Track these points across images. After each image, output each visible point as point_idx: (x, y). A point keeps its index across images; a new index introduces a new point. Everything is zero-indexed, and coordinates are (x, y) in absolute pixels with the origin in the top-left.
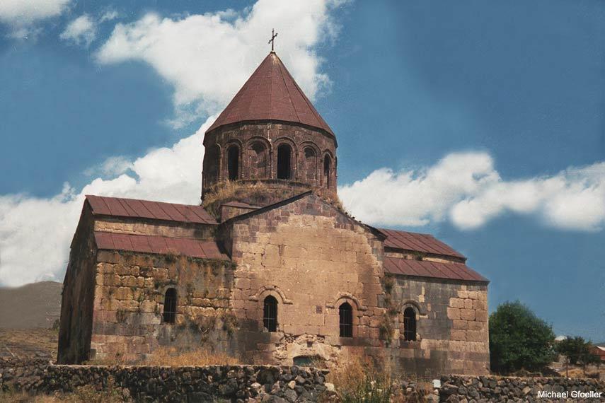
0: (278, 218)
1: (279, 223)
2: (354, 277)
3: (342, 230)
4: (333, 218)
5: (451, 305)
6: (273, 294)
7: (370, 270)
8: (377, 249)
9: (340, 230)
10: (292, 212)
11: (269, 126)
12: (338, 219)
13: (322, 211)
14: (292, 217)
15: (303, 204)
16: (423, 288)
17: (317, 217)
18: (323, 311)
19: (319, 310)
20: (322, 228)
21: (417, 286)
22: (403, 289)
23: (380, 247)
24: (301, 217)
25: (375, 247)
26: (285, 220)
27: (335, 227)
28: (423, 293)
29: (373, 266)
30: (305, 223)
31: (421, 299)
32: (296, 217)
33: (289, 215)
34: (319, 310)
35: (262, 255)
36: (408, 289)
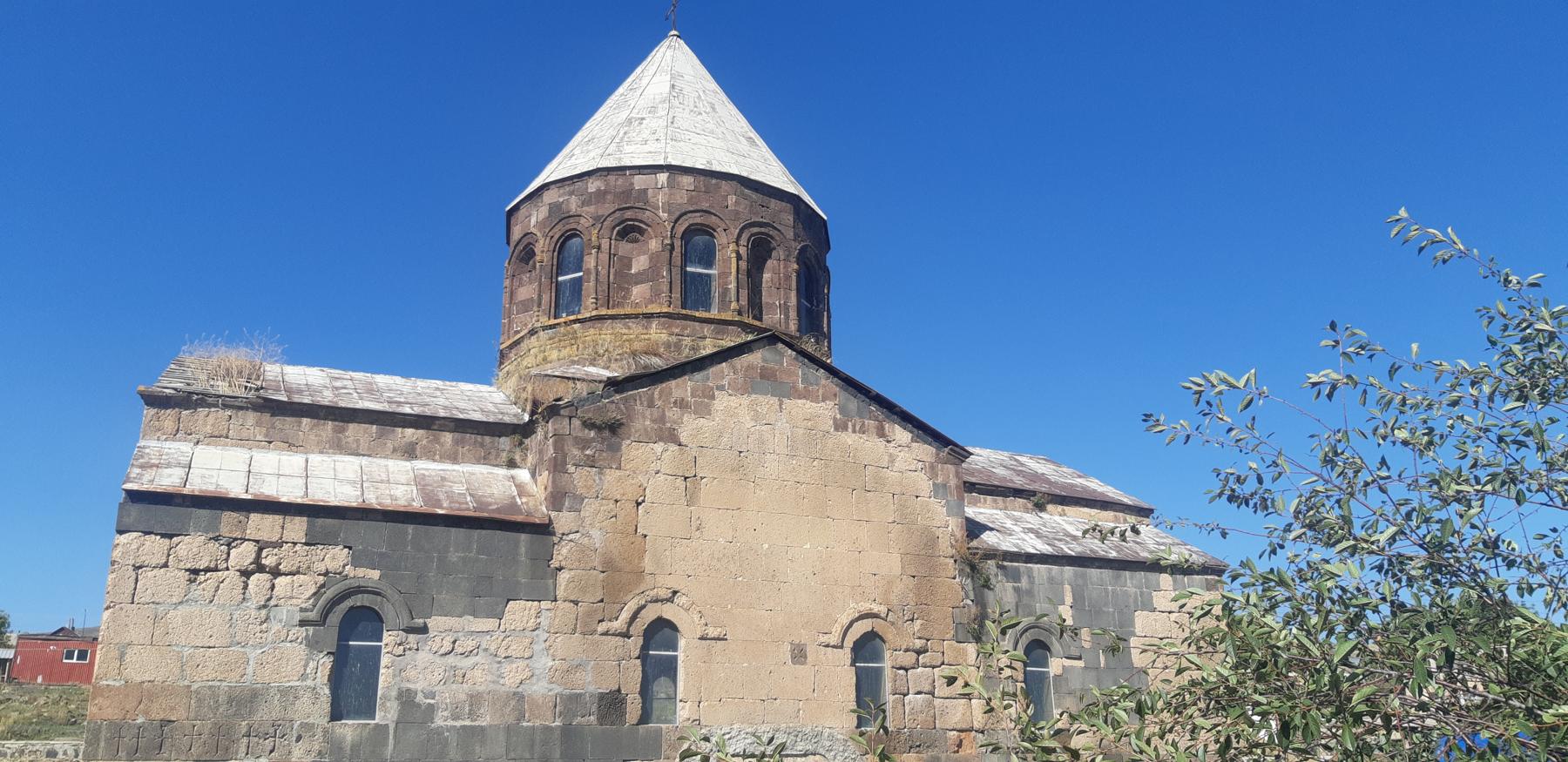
0: (682, 404)
1: (685, 418)
2: (892, 563)
3: (856, 437)
4: (830, 404)
5: (1138, 631)
6: (668, 612)
7: (932, 541)
8: (944, 486)
9: (849, 438)
10: (721, 388)
11: (663, 177)
12: (842, 410)
13: (801, 386)
14: (722, 402)
15: (750, 367)
16: (1067, 588)
17: (786, 400)
18: (809, 659)
19: (799, 654)
20: (801, 431)
21: (1051, 580)
22: (1017, 590)
23: (953, 482)
24: (745, 400)
25: (940, 480)
26: (703, 410)
27: (836, 429)
28: (1069, 599)
29: (939, 533)
30: (756, 417)
31: (1066, 612)
32: (734, 401)
33: (713, 397)
34: (799, 654)
35: (638, 504)
36: (1030, 593)
